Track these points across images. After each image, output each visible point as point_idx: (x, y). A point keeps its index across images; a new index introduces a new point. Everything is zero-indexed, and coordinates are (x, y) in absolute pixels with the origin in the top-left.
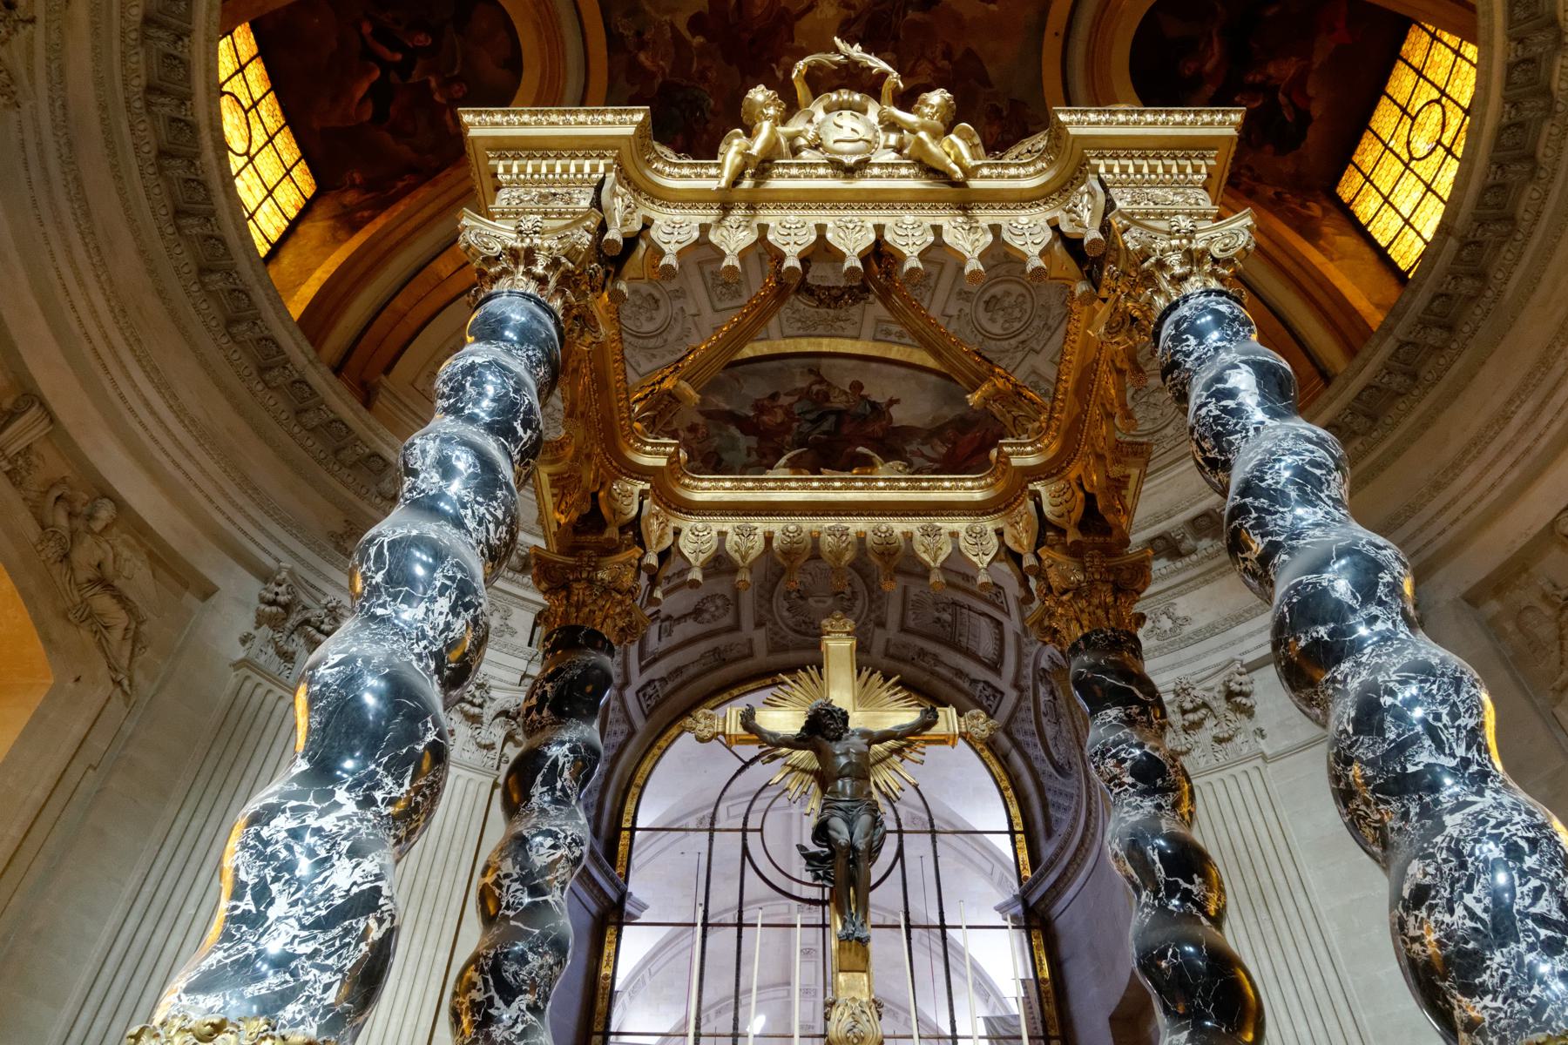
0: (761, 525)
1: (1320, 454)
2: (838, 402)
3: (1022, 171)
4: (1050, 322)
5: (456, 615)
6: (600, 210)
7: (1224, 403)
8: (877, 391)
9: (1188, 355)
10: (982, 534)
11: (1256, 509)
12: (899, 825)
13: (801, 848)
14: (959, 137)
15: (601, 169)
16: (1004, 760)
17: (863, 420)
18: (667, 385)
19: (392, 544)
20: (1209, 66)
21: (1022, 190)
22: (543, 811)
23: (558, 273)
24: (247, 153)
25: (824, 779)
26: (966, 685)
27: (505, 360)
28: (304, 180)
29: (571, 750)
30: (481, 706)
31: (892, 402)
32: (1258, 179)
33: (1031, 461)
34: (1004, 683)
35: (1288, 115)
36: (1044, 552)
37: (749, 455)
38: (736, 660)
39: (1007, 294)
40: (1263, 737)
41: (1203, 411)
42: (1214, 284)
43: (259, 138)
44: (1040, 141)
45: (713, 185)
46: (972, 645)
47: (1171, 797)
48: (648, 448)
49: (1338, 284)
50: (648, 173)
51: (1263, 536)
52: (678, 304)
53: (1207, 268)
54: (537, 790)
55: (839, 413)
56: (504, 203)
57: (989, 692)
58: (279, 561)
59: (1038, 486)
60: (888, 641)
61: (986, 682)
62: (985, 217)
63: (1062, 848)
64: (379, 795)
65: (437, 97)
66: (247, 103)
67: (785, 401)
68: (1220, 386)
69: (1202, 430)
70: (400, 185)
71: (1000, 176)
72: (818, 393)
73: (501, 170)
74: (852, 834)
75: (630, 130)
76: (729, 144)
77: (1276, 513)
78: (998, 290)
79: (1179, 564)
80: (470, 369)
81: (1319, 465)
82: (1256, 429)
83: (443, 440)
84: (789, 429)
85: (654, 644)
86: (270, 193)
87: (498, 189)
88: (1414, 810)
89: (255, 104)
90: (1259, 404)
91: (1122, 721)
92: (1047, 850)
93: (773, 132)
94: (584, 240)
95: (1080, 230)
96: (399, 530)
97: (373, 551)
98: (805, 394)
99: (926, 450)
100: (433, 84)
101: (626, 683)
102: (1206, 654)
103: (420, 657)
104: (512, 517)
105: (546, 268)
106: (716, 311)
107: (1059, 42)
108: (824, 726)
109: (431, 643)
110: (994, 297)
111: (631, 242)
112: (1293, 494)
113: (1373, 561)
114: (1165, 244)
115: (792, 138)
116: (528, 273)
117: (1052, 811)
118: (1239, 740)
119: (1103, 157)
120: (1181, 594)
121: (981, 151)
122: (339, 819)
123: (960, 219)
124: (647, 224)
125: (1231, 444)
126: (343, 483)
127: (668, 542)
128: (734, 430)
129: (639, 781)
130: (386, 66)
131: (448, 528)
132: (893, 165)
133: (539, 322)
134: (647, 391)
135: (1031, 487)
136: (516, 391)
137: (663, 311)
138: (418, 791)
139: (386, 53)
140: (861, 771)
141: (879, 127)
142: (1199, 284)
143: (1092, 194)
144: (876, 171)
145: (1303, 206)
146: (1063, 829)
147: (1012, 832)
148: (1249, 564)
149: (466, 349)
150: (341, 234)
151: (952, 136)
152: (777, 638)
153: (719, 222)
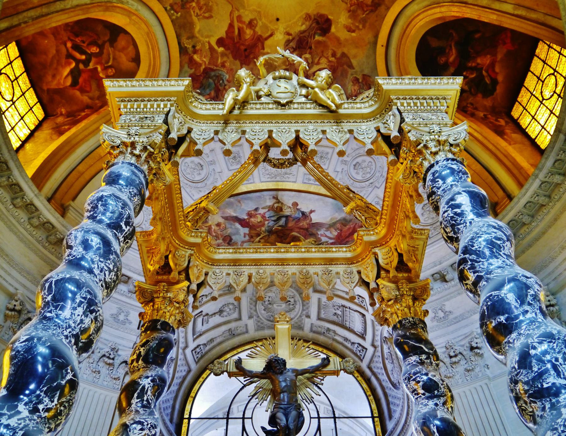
0: (247, 270)
1: (499, 234)
2: (287, 212)
3: (363, 105)
5: (87, 316)
6: (167, 125)
7: (455, 210)
8: (304, 207)
9: (439, 188)
10: (351, 273)
11: (471, 260)
12: (318, 414)
13: (263, 428)
14: (334, 90)
15: (169, 106)
16: (368, 381)
17: (299, 220)
18: (203, 205)
19: (57, 282)
20: (451, 59)
21: (363, 114)
22: (137, 411)
23: (146, 154)
24: (12, 100)
25: (275, 393)
26: (349, 345)
27: (118, 194)
28: (39, 112)
29: (152, 381)
30: (113, 359)
31: (311, 212)
32: (476, 109)
33: (373, 238)
34: (367, 344)
35: (487, 81)
36: (380, 281)
37: (245, 237)
38: (239, 335)
39: (364, 161)
40: (488, 368)
41: (446, 214)
42: (450, 156)
43: (18, 93)
44: (371, 92)
45: (220, 113)
46: (352, 326)
47: (442, 400)
48: (193, 234)
49: (513, 155)
50: (191, 107)
51: (474, 273)
52: (211, 167)
53: (447, 148)
54: (134, 401)
55: (287, 217)
56: (123, 121)
57: (360, 348)
58: (17, 289)
59: (376, 250)
60: (312, 324)
61: (358, 344)
62: (346, 126)
63: (397, 425)
64: (41, 407)
65: (101, 75)
66: (13, 78)
67: (261, 211)
68: (453, 202)
69: (445, 223)
70: (83, 114)
71: (352, 108)
72: (277, 208)
73: (122, 107)
74: (287, 421)
75: (182, 88)
76: (228, 95)
77: (480, 262)
78: (359, 160)
79: (446, 286)
80: (100, 199)
81: (499, 239)
82: (470, 223)
83: (85, 232)
84: (263, 225)
85: (200, 328)
86: (22, 118)
87: (121, 115)
88: (548, 406)
89: (16, 78)
90: (471, 211)
91: (418, 362)
92: (390, 425)
93: (248, 89)
94: (159, 138)
95: (389, 132)
96: (60, 275)
97: (47, 285)
98: (271, 208)
99: (328, 234)
100: (99, 69)
101: (186, 347)
102: (460, 329)
103: (67, 337)
104: (118, 268)
105: (141, 151)
107: (384, 49)
108: (275, 367)
109: (73, 330)
111: (181, 140)
112: (487, 252)
113: (525, 284)
114: (428, 138)
115: (257, 92)
116: (132, 153)
117: (391, 406)
118: (477, 370)
119: (399, 99)
121: (344, 97)
122: (19, 420)
123: (334, 127)
125: (459, 229)
126: (50, 252)
127: (202, 278)
128: (238, 225)
129: (193, 394)
130: (78, 61)
131: (85, 274)
132: (303, 103)
133: (136, 176)
134: (194, 207)
135: (373, 250)
136: (122, 208)
138: (61, 404)
139: (78, 55)
140: (293, 389)
141: (298, 87)
142: (443, 156)
143: (394, 115)
144: (296, 106)
145: (497, 120)
146: (396, 415)
147: (373, 417)
148: (468, 286)
149: (101, 189)
150: (54, 137)
151: (330, 90)
152: (259, 324)
153: (223, 130)
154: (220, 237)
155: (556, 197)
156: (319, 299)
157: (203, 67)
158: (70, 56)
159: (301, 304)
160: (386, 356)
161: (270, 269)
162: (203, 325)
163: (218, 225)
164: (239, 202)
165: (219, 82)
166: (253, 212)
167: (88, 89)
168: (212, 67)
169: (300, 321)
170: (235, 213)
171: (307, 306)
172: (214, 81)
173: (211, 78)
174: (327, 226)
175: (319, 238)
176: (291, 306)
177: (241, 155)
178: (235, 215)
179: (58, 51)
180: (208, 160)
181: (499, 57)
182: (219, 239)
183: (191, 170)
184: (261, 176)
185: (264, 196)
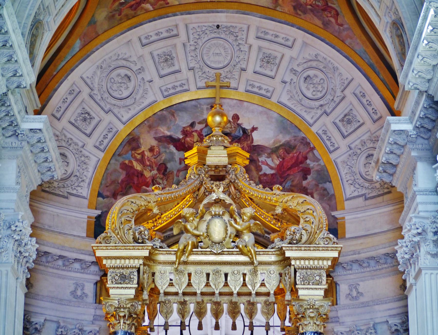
4: (335, 99)
31: (254, 129)
39: (316, 76)
52: (140, 76)
62: (260, 269)
75: (146, 253)
78: (311, 73)
79: (362, 270)
99: (269, 161)
106: (161, 77)
110: (309, 76)
114: (305, 307)
120: (362, 281)
124: (153, 274)
128: (172, 148)
137: (133, 82)
141: (229, 226)
144: (225, 253)
154: (154, 166)
161: (206, 298)
163: (151, 150)
164: (173, 115)
166: (188, 129)
170: (169, 131)
174: (269, 151)
175: (260, 166)
177: (174, 55)
178: (168, 134)
180: (135, 68)
182: (154, 170)
183: (118, 85)
184: (198, 80)
185: (200, 104)
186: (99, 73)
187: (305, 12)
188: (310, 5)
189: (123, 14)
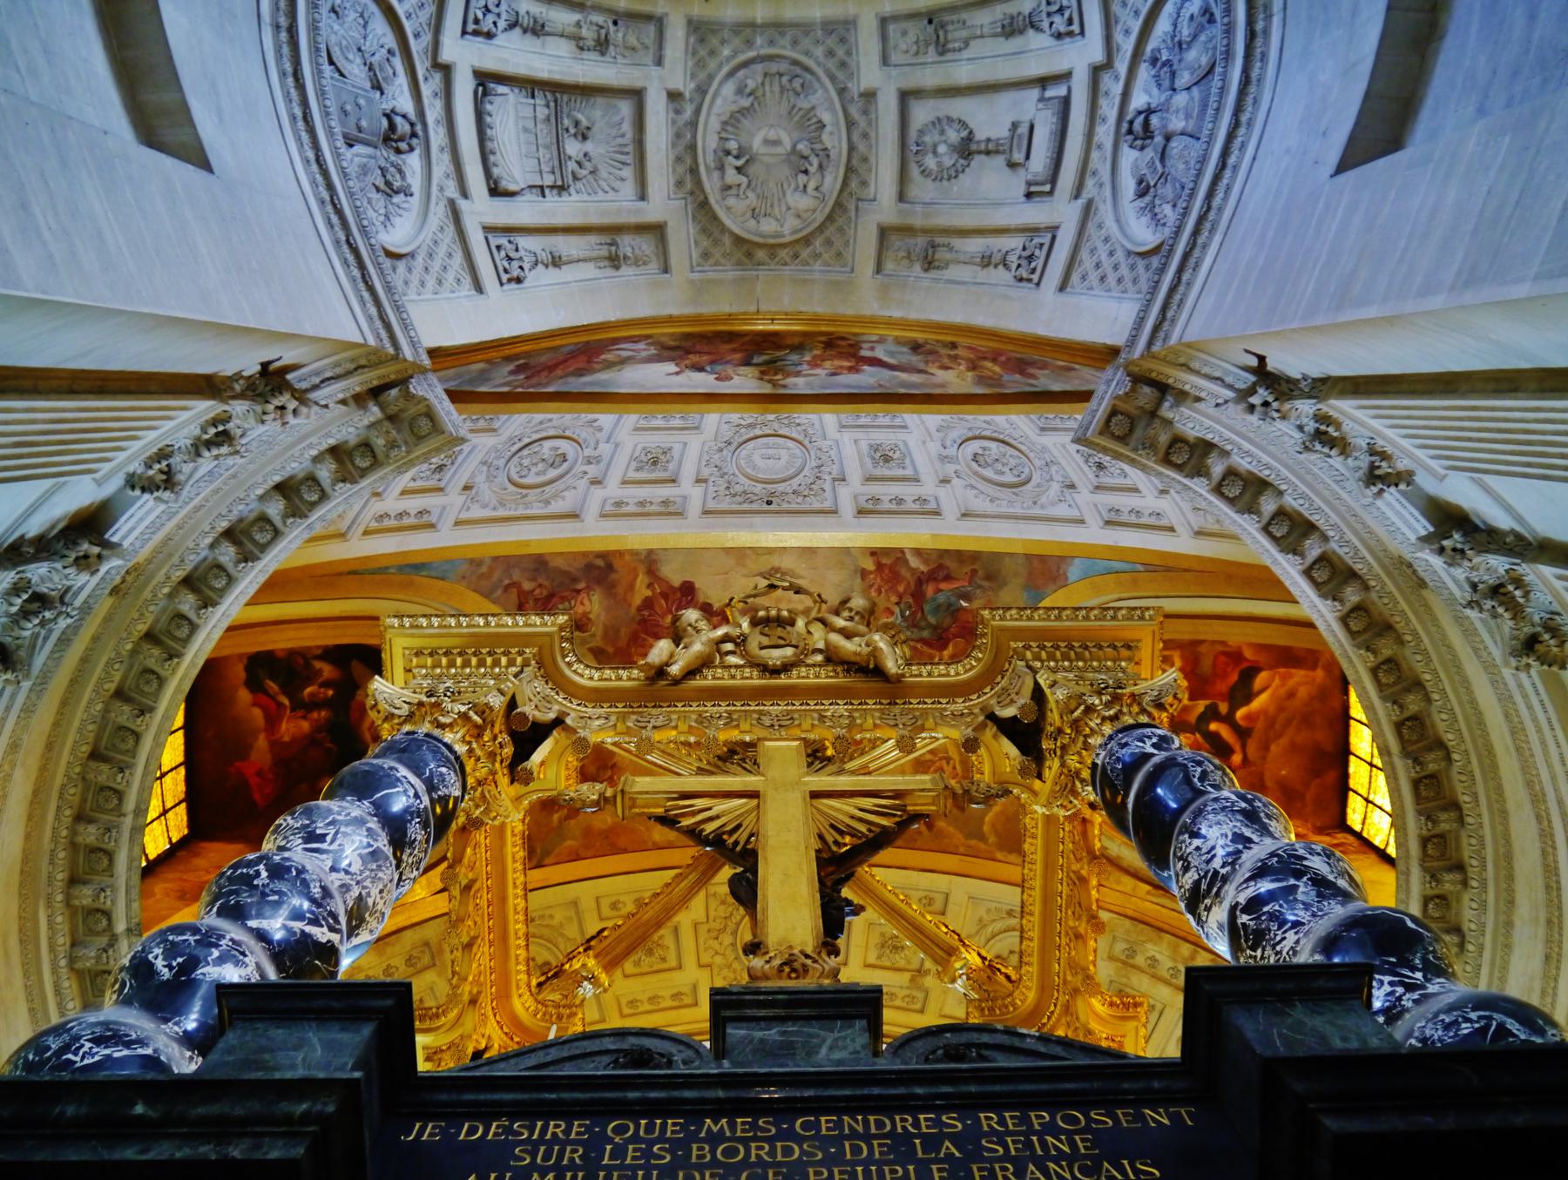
39: (538, 474)
60: (659, 62)
78: (552, 473)
130: (1229, 720)
155: (72, 791)
156: (643, 197)
157: (946, 653)
158: (1243, 733)
159: (700, 152)
160: (397, 62)
162: (1032, 128)
165: (913, 614)
167: (1223, 659)
168: (925, 649)
169: (700, 64)
171: (680, 169)
172: (924, 618)
173: (929, 625)
176: (733, 145)
179: (1265, 748)
181: (262, 742)
186: (1043, 499)
187: (589, 567)
188: (579, 592)
189: (967, 569)
